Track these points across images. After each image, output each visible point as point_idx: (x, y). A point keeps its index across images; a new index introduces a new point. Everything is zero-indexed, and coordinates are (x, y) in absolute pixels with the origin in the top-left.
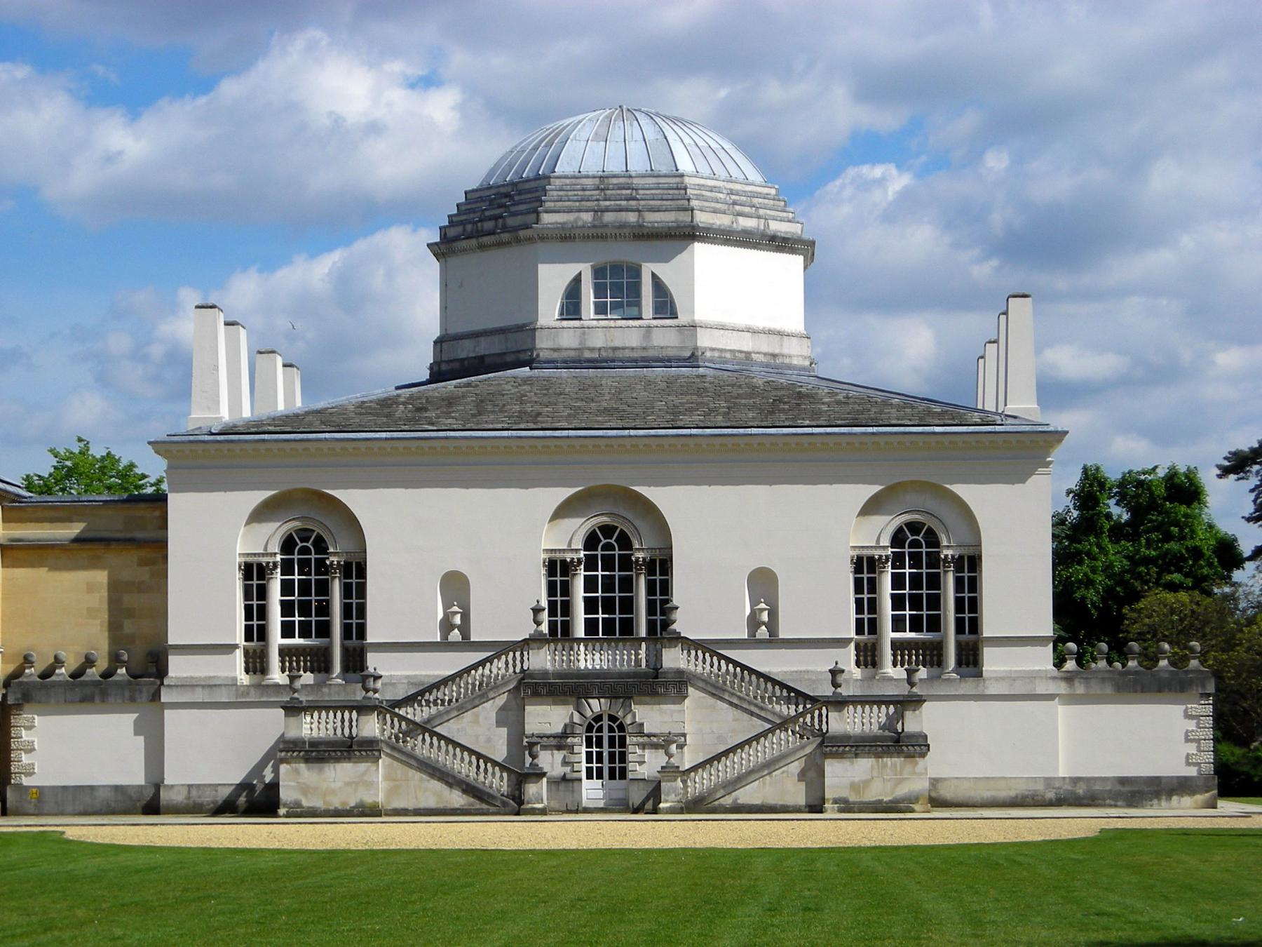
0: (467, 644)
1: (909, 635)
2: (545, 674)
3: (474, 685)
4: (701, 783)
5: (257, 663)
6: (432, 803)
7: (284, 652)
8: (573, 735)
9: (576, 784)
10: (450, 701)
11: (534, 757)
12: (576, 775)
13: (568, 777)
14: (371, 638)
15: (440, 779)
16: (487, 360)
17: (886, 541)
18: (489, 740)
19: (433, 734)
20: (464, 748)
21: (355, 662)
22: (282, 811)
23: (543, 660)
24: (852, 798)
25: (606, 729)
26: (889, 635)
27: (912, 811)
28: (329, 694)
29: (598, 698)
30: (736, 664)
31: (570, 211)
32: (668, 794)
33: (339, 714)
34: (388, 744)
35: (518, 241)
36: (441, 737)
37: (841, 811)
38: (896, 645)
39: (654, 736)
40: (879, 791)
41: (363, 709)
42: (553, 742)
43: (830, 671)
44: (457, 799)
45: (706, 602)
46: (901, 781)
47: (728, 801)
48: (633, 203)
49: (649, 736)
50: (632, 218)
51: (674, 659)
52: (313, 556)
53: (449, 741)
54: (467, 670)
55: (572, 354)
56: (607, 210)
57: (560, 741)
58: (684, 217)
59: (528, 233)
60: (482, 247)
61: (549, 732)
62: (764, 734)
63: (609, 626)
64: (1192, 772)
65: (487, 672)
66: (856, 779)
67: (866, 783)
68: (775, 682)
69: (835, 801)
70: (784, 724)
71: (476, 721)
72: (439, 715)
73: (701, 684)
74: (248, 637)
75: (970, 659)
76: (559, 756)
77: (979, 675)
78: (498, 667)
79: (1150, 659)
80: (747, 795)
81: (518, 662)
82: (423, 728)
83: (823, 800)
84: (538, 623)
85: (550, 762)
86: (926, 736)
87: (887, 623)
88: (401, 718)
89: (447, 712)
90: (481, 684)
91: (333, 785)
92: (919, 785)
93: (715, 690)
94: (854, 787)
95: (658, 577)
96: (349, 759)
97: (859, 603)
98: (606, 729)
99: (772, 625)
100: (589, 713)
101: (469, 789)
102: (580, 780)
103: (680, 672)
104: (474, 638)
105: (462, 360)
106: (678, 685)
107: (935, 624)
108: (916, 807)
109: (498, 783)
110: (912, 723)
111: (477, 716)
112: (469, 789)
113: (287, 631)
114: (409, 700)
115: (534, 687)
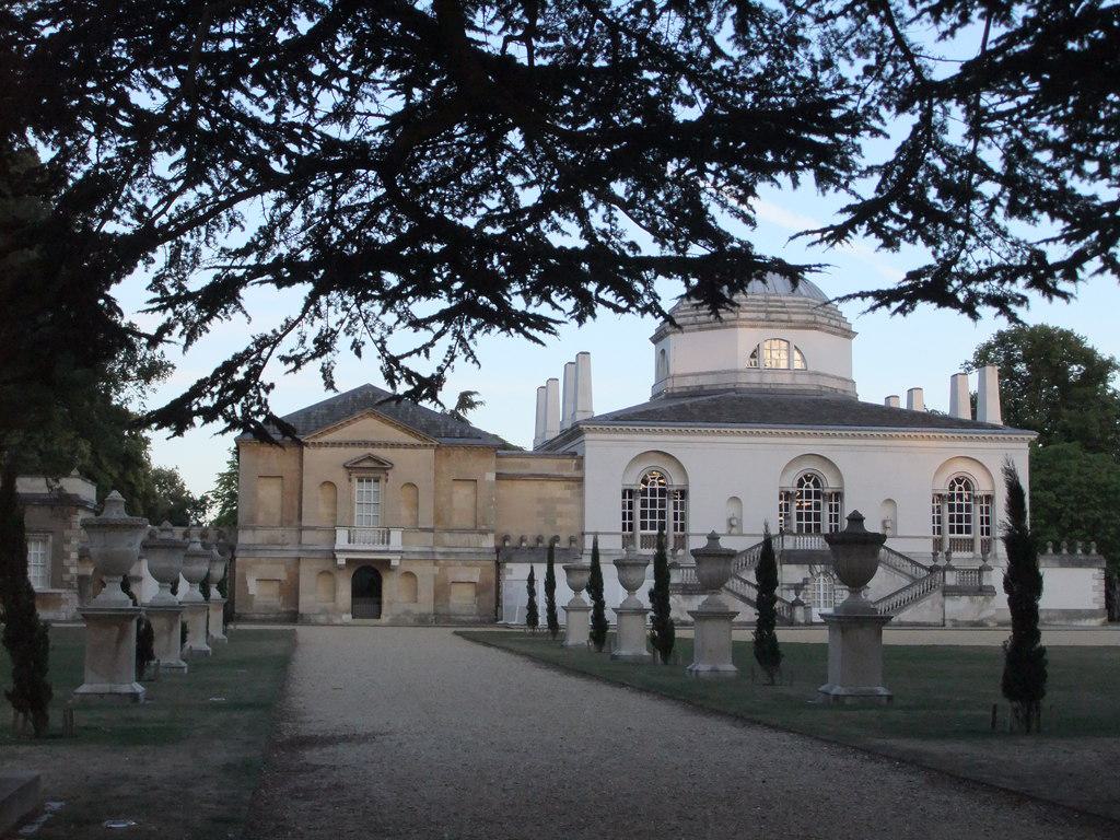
1: (956, 535)
8: (807, 584)
16: (706, 388)
26: (948, 536)
31: (754, 312)
35: (726, 327)
40: (971, 616)
48: (784, 309)
50: (785, 317)
55: (756, 386)
56: (772, 312)
58: (811, 318)
59: (732, 323)
60: (700, 329)
63: (809, 528)
64: (1097, 607)
68: (907, 559)
79: (1072, 551)
87: (947, 529)
105: (688, 388)
107: (968, 530)
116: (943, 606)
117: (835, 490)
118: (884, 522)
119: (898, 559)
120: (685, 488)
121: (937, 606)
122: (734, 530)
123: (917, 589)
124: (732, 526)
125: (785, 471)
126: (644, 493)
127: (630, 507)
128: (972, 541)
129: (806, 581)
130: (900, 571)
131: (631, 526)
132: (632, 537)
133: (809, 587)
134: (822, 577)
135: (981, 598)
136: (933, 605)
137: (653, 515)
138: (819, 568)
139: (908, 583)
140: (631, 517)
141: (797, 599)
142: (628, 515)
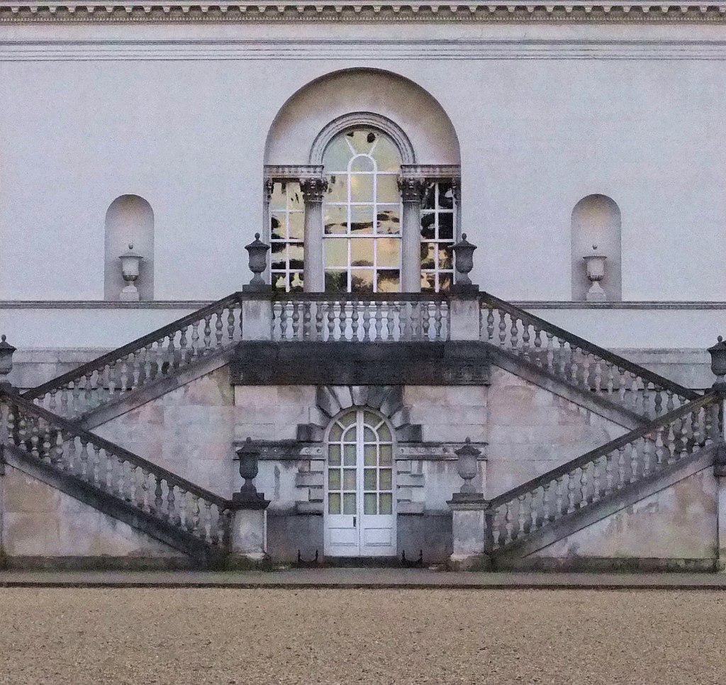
3: (154, 365)
4: (517, 515)
6: (84, 548)
8: (310, 442)
9: (314, 519)
10: (118, 389)
11: (249, 475)
13: (302, 508)
15: (100, 508)
18: (178, 451)
19: (88, 438)
23: (258, 324)
25: (360, 432)
29: (350, 386)
32: (465, 539)
36: (100, 443)
39: (437, 445)
43: (711, 351)
44: (123, 539)
47: (559, 551)
49: (429, 445)
51: (464, 325)
57: (289, 452)
61: (272, 439)
62: (617, 444)
65: (177, 344)
70: (644, 426)
71: (158, 421)
72: (103, 408)
73: (512, 367)
76: (288, 475)
78: (195, 336)
80: (593, 539)
82: (79, 428)
84: (257, 270)
85: (278, 484)
89: (114, 405)
90: (166, 365)
93: (534, 369)
98: (360, 432)
100: (334, 410)
102: (320, 514)
104: (158, 296)
111: (159, 412)
114: (56, 384)
115: (254, 365)
117: (437, 173)
119: (600, 365)
121: (695, 509)
123: (641, 452)
125: (284, 117)
129: (306, 435)
130: (607, 404)
133: (313, 451)
134: (360, 423)
136: (683, 503)
139: (617, 432)
141: (249, 490)
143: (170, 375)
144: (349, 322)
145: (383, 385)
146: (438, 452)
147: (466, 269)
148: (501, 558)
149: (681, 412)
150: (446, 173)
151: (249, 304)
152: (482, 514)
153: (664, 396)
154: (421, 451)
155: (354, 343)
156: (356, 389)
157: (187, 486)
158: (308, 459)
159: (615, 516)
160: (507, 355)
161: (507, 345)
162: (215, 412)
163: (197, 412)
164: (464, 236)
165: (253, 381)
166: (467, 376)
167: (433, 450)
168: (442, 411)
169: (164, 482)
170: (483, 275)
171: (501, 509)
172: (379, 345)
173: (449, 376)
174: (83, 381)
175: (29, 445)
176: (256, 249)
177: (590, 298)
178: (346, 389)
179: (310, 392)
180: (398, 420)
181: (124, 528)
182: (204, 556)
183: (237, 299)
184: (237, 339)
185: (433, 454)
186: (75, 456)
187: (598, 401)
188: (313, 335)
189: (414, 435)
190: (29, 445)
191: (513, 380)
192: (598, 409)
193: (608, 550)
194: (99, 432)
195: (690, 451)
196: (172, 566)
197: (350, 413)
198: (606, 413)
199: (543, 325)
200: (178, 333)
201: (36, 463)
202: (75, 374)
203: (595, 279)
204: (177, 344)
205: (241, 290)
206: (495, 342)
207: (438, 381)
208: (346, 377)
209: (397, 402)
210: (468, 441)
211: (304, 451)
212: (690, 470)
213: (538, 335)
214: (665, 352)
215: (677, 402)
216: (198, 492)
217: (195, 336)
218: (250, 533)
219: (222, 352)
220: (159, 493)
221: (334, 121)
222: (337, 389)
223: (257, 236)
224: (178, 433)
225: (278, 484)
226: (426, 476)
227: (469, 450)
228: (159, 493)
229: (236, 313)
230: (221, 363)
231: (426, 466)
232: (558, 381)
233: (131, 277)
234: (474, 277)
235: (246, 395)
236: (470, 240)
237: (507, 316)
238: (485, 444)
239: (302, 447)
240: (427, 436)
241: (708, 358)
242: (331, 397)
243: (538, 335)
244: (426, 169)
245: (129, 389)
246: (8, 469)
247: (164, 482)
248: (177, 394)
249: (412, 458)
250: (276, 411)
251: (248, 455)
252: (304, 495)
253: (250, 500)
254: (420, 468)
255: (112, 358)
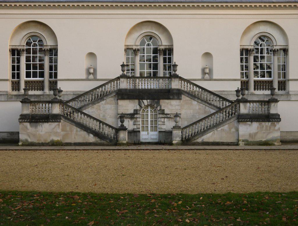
0: (95, 79)
2: (126, 90)
3: (98, 95)
4: (189, 132)
5: (16, 86)
7: (26, 82)
8: (137, 114)
9: (138, 133)
10: (89, 101)
11: (122, 122)
12: (138, 130)
13: (135, 130)
14: (59, 77)
17: (253, 44)
18: (104, 116)
19: (82, 113)
20: (94, 119)
21: (53, 85)
22: (20, 144)
23: (124, 84)
24: (250, 140)
25: (149, 111)
27: (274, 145)
28: (43, 98)
29: (147, 100)
30: (200, 87)
32: (176, 137)
33: (44, 105)
34: (63, 116)
37: (246, 145)
38: (255, 82)
39: (168, 114)
41: (52, 102)
42: (130, 116)
43: (236, 91)
44: (91, 138)
45: (188, 65)
46: (269, 133)
47: (200, 140)
49: (166, 114)
51: (175, 85)
52: (38, 47)
53: (88, 116)
54: (96, 89)
57: (132, 116)
61: (127, 113)
65: (104, 90)
66: (252, 132)
67: (256, 134)
69: (243, 141)
72: (85, 106)
73: (186, 95)
74: (13, 77)
75: (283, 85)
77: (288, 94)
80: (208, 137)
81: (115, 86)
82: (79, 110)
83: (238, 140)
84: (123, 71)
85: (129, 124)
86: (279, 115)
88: (70, 107)
89: (88, 105)
90: (101, 95)
91: (41, 133)
92: (275, 135)
93: (192, 96)
94: (250, 135)
95: (167, 56)
96: (48, 122)
97: (242, 66)
98: (149, 111)
99: (210, 73)
100: (143, 106)
101: (96, 134)
102: (139, 132)
103: (179, 90)
104: (98, 78)
106: (177, 94)
108: (276, 143)
109: (107, 131)
110: (274, 109)
111: (100, 106)
112: (96, 134)
113: (28, 75)
115: (123, 95)
116: (237, 130)
117: (167, 47)
118: (203, 70)
119: (209, 94)
120: (56, 47)
121: (233, 130)
122: (91, 77)
123: (220, 116)
124: (90, 73)
125: (130, 33)
126: (28, 51)
127: (19, 62)
128: (271, 82)
129: (136, 112)
130: (210, 104)
131: (18, 75)
132: (18, 83)
133: (138, 116)
134: (149, 109)
135: (268, 124)
136: (230, 129)
137: (35, 67)
138: (146, 102)
139: (213, 111)
140: (19, 68)
141: (122, 126)
142: (16, 69)
143: (102, 97)
144: (146, 84)
145: (155, 99)
146: (169, 116)
147: (175, 71)
148: (186, 141)
149: (229, 106)
150: (284, 47)
151: (122, 80)
152: (180, 131)
153: (224, 102)
154: (165, 116)
155: (148, 89)
156: (148, 100)
157: (107, 125)
158: (137, 118)
159: (213, 132)
160: (186, 92)
161: (186, 90)
162: (113, 107)
163: (108, 106)
164: (175, 63)
165: (123, 98)
166: (176, 97)
167: (168, 115)
168: (170, 106)
169: (101, 124)
170: (179, 72)
171: (185, 130)
172: (155, 90)
173: (171, 97)
174: (80, 99)
175: (67, 114)
176: (123, 66)
177: (205, 78)
178: (146, 100)
179: (137, 101)
180: (159, 108)
181: (91, 135)
182: (115, 142)
183: (118, 78)
184: (118, 88)
185: (167, 116)
186: (78, 117)
187: (208, 103)
188: (137, 87)
189: (162, 112)
190: (67, 114)
191: (188, 98)
192: (208, 105)
193: (211, 140)
194: (84, 111)
195: (232, 116)
196: (103, 145)
197: (147, 106)
198: (210, 106)
199: (194, 85)
200: (104, 87)
201: (69, 119)
202: (78, 97)
203: (207, 73)
204: (104, 90)
205: (119, 76)
206: (183, 89)
207: (169, 98)
208: (146, 98)
209: (158, 104)
210: (177, 113)
211: (135, 116)
212: (232, 120)
213: (193, 87)
214: (224, 91)
215: (228, 104)
216: (110, 126)
217: (108, 88)
218: (123, 136)
219: (115, 91)
220: (100, 127)
221: (142, 34)
222: (144, 101)
223: (123, 63)
224: (104, 112)
225: (129, 124)
226: (166, 122)
227: (177, 115)
228: (100, 127)
229: (118, 82)
230: (115, 94)
231: (166, 119)
232: (198, 99)
233: (92, 73)
234: (177, 73)
235: (121, 102)
236: (176, 64)
237: (186, 82)
238: (180, 114)
239: (135, 115)
240: (166, 112)
241: (235, 93)
242: (142, 102)
243: (193, 87)
244: (165, 46)
245: (92, 101)
246: (62, 121)
247: (101, 124)
248: (103, 102)
249: (162, 118)
250: (128, 106)
251: (122, 117)
252: (135, 127)
253: (123, 128)
254: (164, 120)
255: (87, 93)
